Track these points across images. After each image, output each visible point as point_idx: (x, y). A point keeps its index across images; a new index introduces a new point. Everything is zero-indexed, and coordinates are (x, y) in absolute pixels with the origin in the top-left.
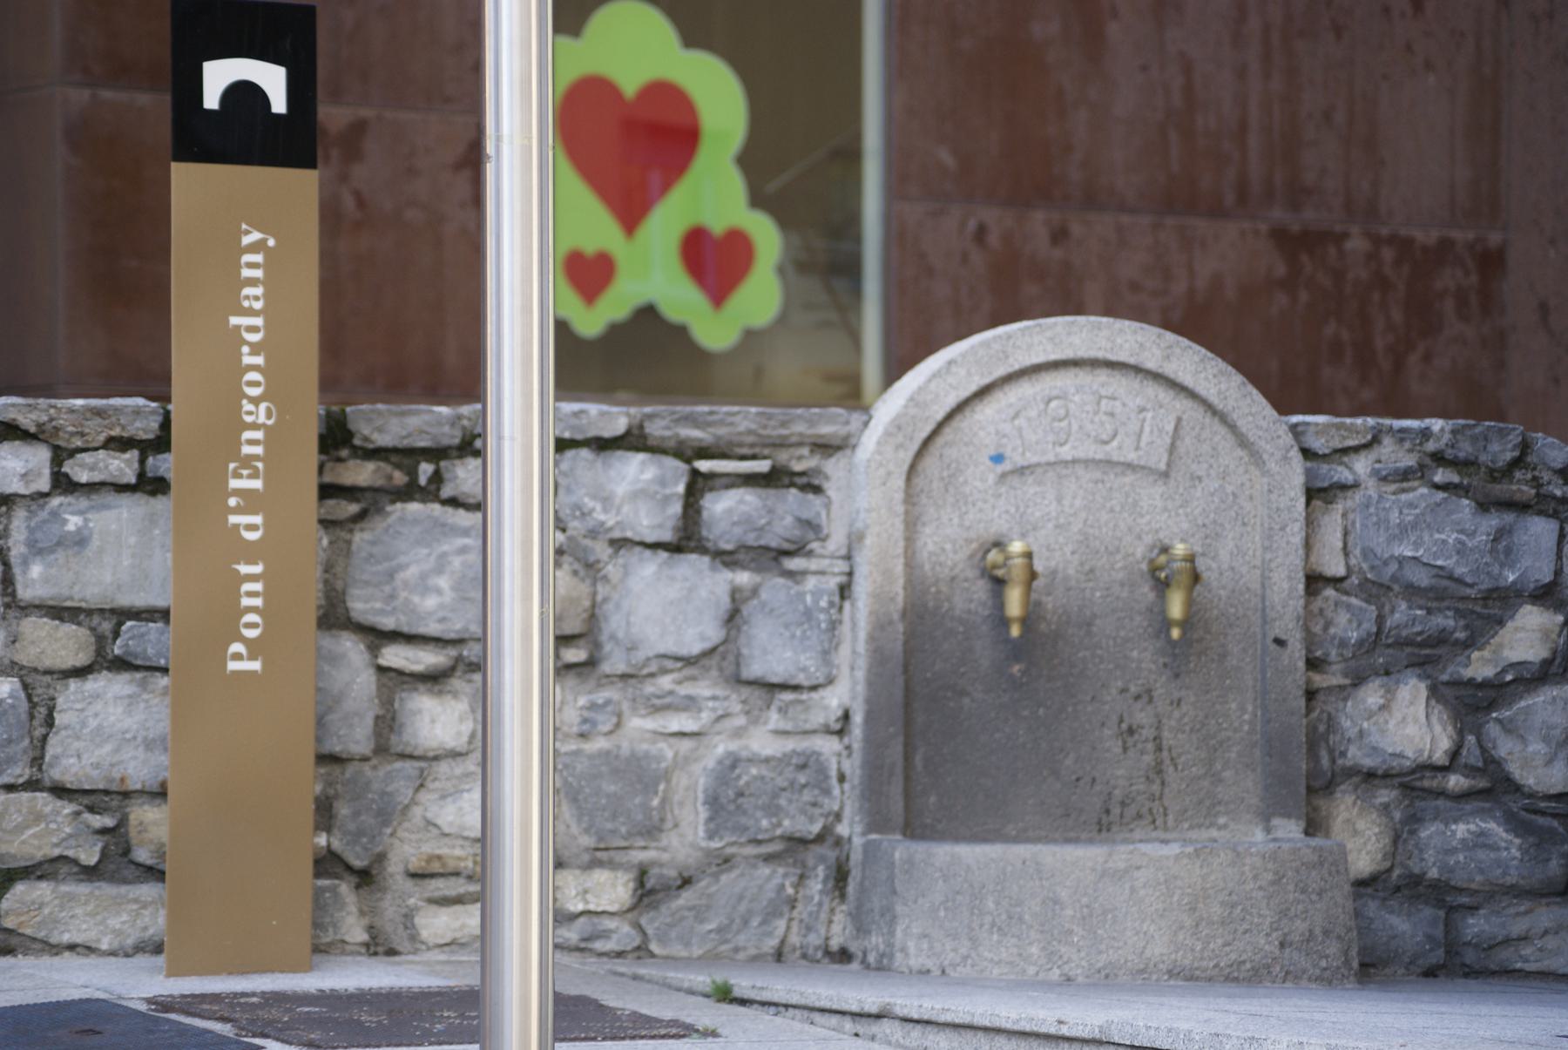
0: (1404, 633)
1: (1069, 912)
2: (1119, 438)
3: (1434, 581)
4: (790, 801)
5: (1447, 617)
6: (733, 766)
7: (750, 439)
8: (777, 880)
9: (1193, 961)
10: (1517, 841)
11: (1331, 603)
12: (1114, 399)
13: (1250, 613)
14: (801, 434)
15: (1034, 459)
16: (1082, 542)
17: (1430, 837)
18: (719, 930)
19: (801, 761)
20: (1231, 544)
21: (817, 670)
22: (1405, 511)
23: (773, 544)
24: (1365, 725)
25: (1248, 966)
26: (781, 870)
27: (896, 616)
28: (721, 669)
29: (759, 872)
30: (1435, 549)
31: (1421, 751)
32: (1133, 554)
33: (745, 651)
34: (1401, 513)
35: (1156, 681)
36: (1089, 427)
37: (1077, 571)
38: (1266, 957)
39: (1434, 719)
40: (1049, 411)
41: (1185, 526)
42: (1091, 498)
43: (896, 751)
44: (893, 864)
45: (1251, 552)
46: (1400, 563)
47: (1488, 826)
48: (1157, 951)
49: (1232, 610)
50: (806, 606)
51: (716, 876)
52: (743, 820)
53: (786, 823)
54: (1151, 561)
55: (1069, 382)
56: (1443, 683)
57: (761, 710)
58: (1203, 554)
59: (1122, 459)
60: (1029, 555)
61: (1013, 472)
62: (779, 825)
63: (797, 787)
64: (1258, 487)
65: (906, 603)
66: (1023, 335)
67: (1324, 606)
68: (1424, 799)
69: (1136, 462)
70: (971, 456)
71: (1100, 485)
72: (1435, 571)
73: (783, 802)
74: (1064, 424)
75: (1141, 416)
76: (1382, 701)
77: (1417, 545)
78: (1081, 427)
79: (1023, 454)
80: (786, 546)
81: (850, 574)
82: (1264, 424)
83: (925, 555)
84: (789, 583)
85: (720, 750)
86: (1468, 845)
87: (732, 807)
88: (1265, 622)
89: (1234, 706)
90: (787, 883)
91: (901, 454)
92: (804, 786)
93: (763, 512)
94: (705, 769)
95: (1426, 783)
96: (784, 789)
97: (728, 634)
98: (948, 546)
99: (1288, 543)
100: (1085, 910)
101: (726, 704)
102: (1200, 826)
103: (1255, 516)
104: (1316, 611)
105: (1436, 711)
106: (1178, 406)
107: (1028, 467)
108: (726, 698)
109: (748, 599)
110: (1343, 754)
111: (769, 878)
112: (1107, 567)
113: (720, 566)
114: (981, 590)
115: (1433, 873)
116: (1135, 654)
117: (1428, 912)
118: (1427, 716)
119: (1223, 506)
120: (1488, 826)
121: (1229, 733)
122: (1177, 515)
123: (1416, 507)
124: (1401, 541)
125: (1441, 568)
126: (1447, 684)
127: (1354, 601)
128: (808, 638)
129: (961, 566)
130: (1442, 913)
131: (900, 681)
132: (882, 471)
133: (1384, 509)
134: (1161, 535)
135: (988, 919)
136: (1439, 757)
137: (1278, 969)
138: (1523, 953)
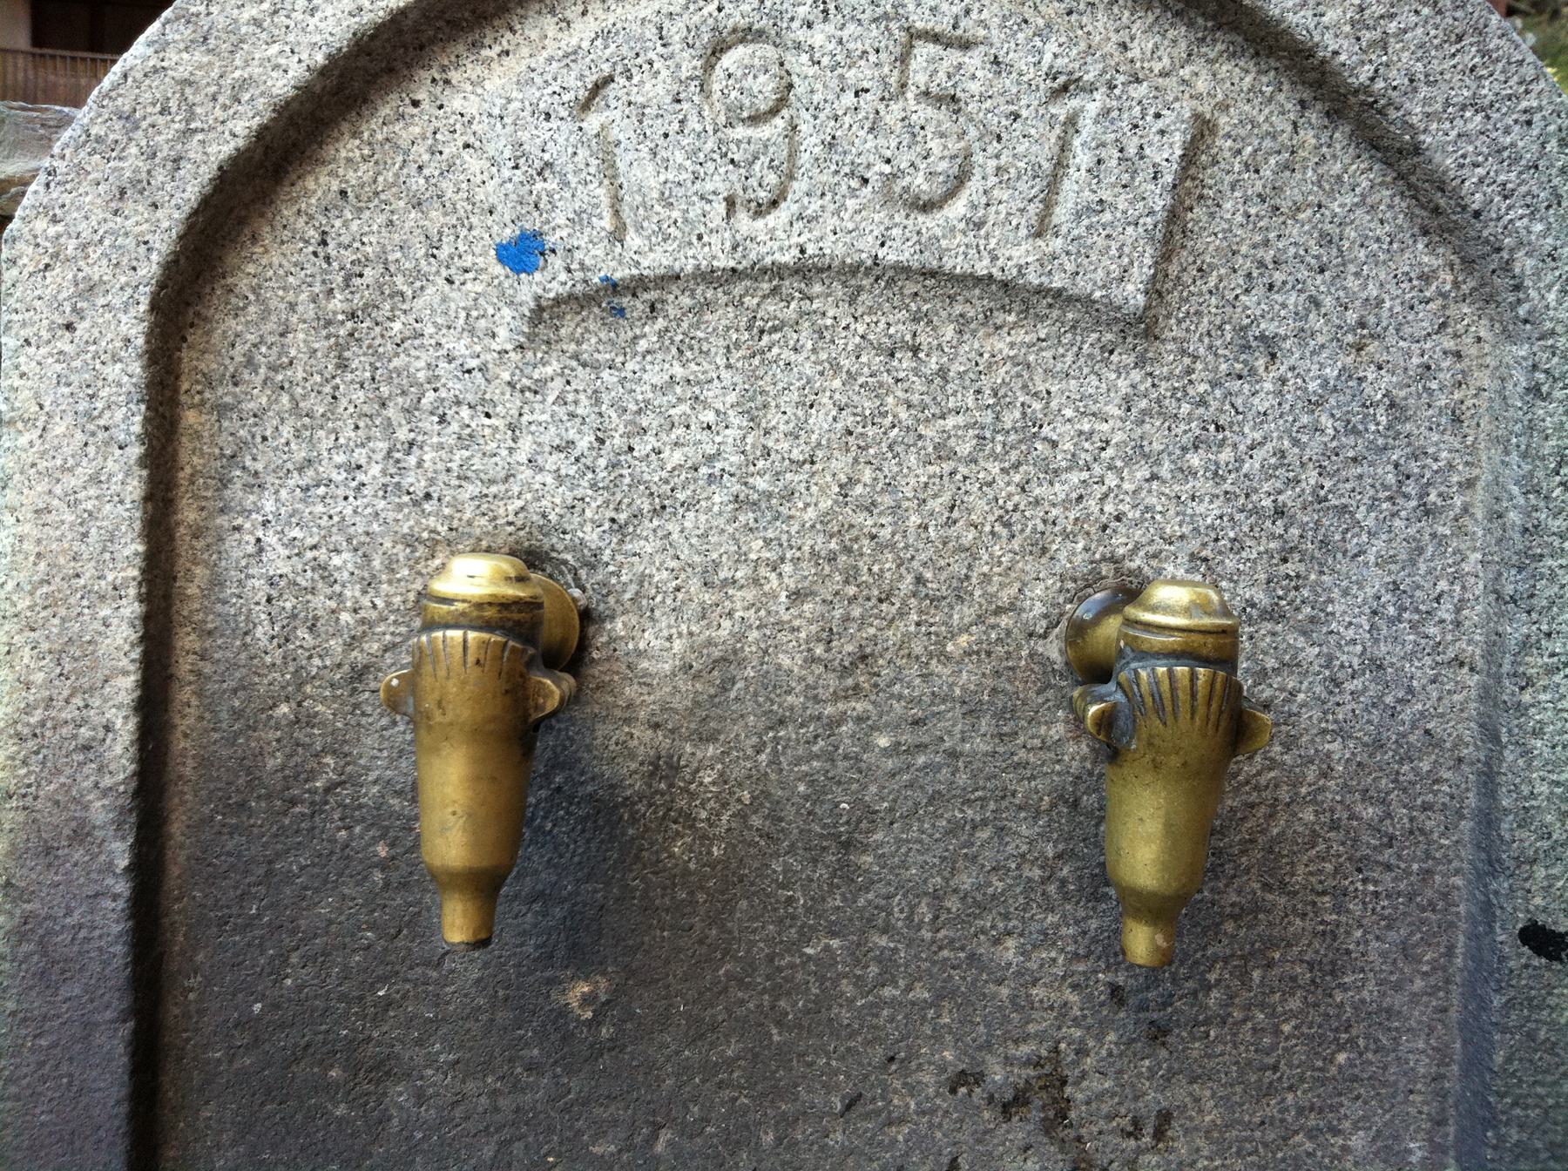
2: (974, 186)
12: (966, 45)
13: (1431, 823)
15: (656, 260)
16: (832, 558)
20: (1376, 581)
27: (100, 812)
32: (1012, 607)
35: (1082, 1052)
37: (813, 660)
40: (717, 83)
41: (1209, 511)
42: (868, 405)
45: (1445, 612)
49: (1370, 812)
54: (1078, 631)
58: (1272, 614)
59: (982, 268)
64: (1483, 379)
69: (1033, 279)
70: (433, 246)
71: (904, 361)
74: (764, 132)
75: (1061, 110)
79: (617, 235)
82: (1526, 143)
88: (1490, 865)
89: (1358, 1141)
91: (136, 216)
103: (1470, 484)
106: (1202, 85)
107: (637, 285)
116: (1010, 951)
119: (1352, 446)
129: (386, 632)
131: (114, 1043)
132: (62, 277)
134: (1120, 544)
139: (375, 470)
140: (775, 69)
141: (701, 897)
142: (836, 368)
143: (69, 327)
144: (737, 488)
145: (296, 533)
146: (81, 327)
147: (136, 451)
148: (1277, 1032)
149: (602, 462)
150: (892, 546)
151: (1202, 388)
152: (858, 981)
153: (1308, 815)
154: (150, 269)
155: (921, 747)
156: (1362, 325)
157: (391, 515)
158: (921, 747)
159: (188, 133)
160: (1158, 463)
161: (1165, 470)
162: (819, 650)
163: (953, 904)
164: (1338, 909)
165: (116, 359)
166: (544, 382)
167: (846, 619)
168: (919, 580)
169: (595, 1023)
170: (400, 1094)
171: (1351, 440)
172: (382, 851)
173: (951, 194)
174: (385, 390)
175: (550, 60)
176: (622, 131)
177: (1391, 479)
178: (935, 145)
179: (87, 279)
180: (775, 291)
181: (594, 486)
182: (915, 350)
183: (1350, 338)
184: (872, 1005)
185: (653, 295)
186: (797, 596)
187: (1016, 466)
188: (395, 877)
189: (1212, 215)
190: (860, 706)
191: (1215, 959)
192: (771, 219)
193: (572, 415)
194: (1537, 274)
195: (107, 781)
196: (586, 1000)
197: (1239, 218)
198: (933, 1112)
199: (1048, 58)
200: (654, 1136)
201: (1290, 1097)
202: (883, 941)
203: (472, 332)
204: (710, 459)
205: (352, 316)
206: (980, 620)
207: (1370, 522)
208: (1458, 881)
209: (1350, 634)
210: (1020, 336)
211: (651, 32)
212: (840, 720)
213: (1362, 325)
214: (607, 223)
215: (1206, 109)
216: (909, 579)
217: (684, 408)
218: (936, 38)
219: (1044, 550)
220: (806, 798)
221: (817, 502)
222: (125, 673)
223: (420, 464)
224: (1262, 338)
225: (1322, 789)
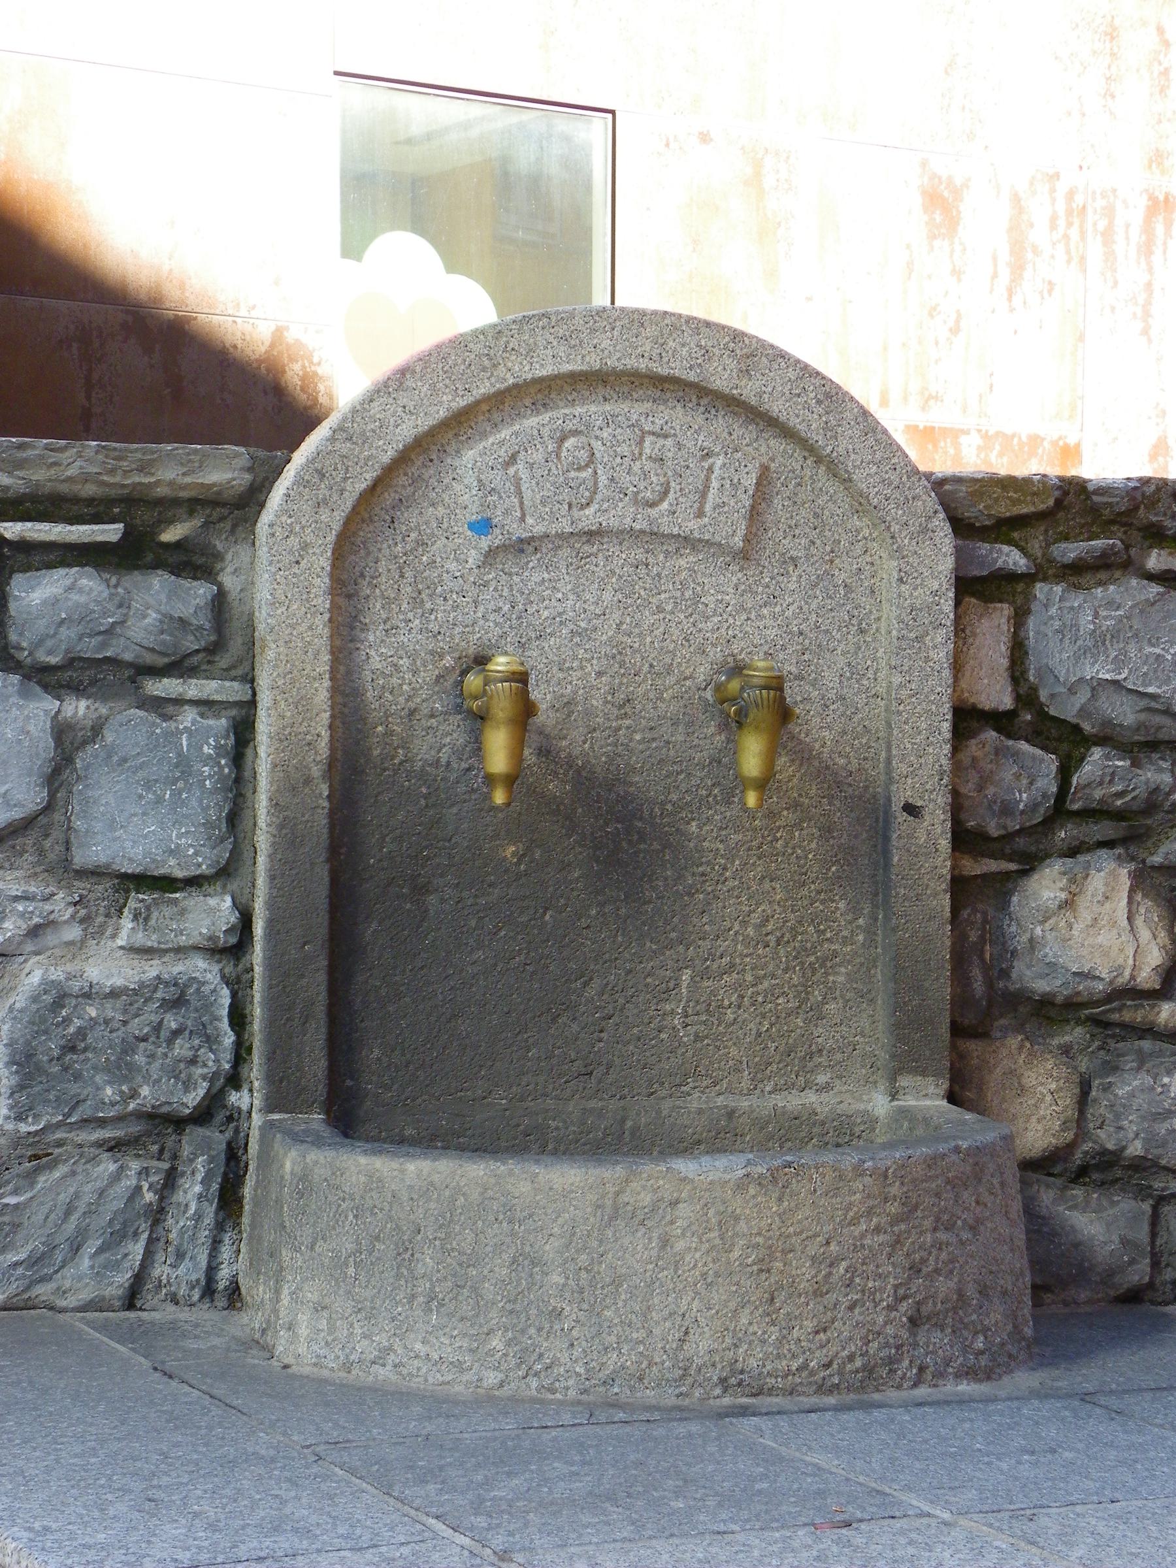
0: (1098, 794)
1: (557, 1278)
2: (671, 496)
3: (1143, 717)
4: (152, 1056)
5: (1161, 770)
6: (58, 1004)
7: (90, 490)
8: (129, 1181)
9: (764, 1360)
12: (666, 436)
14: (171, 483)
15: (539, 530)
17: (1132, 1095)
18: (35, 1261)
19: (171, 993)
20: (841, 662)
21: (196, 854)
22: (1103, 613)
23: (128, 656)
24: (1038, 931)
25: (858, 1363)
26: (135, 1165)
27: (316, 771)
28: (41, 852)
29: (101, 1168)
31: (1120, 969)
33: (78, 824)
34: (1096, 615)
36: (625, 480)
38: (887, 1345)
39: (1139, 921)
41: (772, 633)
43: (316, 984)
44: (282, 1177)
45: (870, 675)
46: (1093, 689)
48: (704, 1346)
49: (842, 761)
50: (180, 754)
51: (30, 1177)
52: (74, 1088)
53: (145, 1091)
54: (719, 688)
55: (593, 408)
56: (1153, 867)
57: (108, 916)
58: (799, 677)
59: (676, 531)
60: (521, 678)
61: (504, 548)
62: (134, 1094)
63: (164, 1034)
65: (333, 749)
66: (520, 331)
67: (979, 754)
68: (1123, 1039)
69: (696, 535)
71: (642, 571)
72: (1143, 703)
73: (140, 1059)
74: (584, 474)
75: (706, 465)
76: (1063, 896)
77: (1119, 663)
78: (612, 479)
79: (523, 519)
80: (149, 659)
81: (252, 703)
82: (893, 476)
83: (367, 673)
84: (153, 718)
85: (36, 978)
87: (55, 1069)
89: (842, 905)
90: (146, 1186)
91: (325, 516)
92: (176, 1033)
93: (110, 606)
94: (11, 1009)
95: (1127, 1016)
96: (144, 1039)
97: (52, 795)
98: (404, 662)
99: (927, 659)
100: (583, 1274)
101: (48, 907)
102: (788, 1087)
103: (879, 619)
105: (1142, 911)
108: (47, 898)
109: (85, 743)
110: (1005, 974)
111: (117, 1177)
112: (652, 695)
113: (38, 689)
114: (454, 733)
115: (1136, 1149)
121: (836, 947)
122: (760, 617)
123: (1118, 609)
125: (1153, 697)
126: (1160, 868)
127: (1024, 746)
128: (183, 803)
130: (1146, 1207)
131: (322, 873)
132: (294, 542)
133: (1072, 608)
134: (735, 648)
135: (423, 1286)
136: (1147, 977)
137: (906, 1363)
139: (417, 622)
140: (587, 448)
141: (562, 808)
142: (613, 572)
143: (297, 562)
144: (572, 627)
145: (383, 650)
146: (303, 563)
147: (327, 616)
148: (806, 857)
149: (514, 616)
150: (639, 651)
151: (767, 580)
152: (630, 842)
153: (816, 763)
154: (331, 538)
155: (654, 739)
156: (832, 552)
157: (424, 642)
158: (654, 739)
159: (345, 479)
160: (750, 613)
161: (753, 616)
162: (609, 698)
163: (669, 807)
164: (830, 804)
165: (319, 576)
166: (488, 582)
167: (621, 684)
168: (651, 666)
169: (518, 863)
170: (432, 899)
171: (829, 601)
172: (424, 790)
173: (662, 500)
174: (420, 586)
175: (493, 444)
176: (524, 475)
177: (846, 617)
178: (654, 479)
179: (305, 542)
180: (588, 541)
181: (511, 627)
182: (647, 565)
183: (827, 558)
184: (635, 852)
185: (537, 544)
186: (599, 674)
187: (691, 615)
188: (431, 801)
189: (769, 506)
190: (628, 722)
191: (779, 827)
192: (587, 512)
193: (501, 596)
194: (900, 531)
195: (318, 758)
196: (514, 854)
197: (780, 507)
198: (663, 897)
199: (700, 442)
200: (545, 913)
201: (813, 887)
202: (639, 824)
203: (457, 561)
204: (560, 614)
205: (405, 554)
206: (678, 682)
207: (838, 636)
208: (879, 790)
209: (831, 685)
210: (691, 559)
211: (535, 432)
212: (619, 729)
213: (832, 552)
214: (518, 514)
215: (765, 460)
216: (647, 665)
217: (549, 592)
218: (654, 434)
219: (704, 652)
220: (606, 763)
222: (325, 711)
223: (436, 618)
224: (791, 558)
225: (822, 753)
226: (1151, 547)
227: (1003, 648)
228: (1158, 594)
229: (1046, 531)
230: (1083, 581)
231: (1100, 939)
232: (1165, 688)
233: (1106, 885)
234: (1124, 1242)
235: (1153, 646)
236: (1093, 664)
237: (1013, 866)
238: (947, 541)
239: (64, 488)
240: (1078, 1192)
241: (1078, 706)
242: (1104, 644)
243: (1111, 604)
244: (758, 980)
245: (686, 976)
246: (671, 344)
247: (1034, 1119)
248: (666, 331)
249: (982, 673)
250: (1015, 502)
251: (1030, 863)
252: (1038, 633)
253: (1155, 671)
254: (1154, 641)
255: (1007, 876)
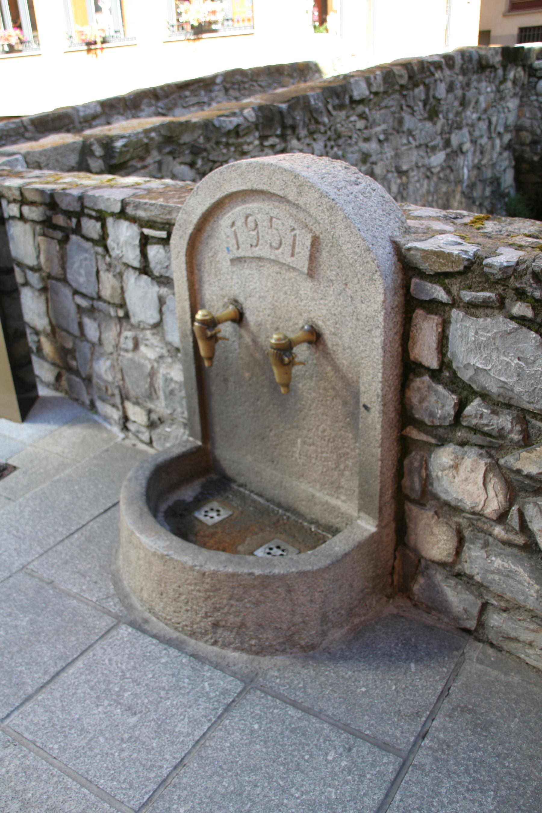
0: (474, 422)
2: (283, 246)
3: (501, 390)
10: (537, 587)
11: (426, 384)
17: (477, 557)
20: (350, 331)
22: (481, 333)
24: (440, 474)
30: (500, 367)
31: (477, 504)
34: (476, 333)
39: (490, 487)
41: (324, 312)
46: (475, 370)
47: (516, 568)
75: (293, 233)
77: (487, 360)
79: (238, 248)
82: (358, 251)
86: (498, 572)
89: (351, 435)
95: (480, 524)
99: (373, 342)
104: (416, 387)
117: (471, 598)
118: (485, 484)
120: (516, 568)
121: (348, 451)
123: (488, 332)
124: (476, 354)
127: (440, 388)
133: (466, 326)
134: (312, 315)
138: (527, 651)
161: (318, 303)
221: (269, 299)
226: (517, 300)
227: (434, 338)
228: (513, 328)
229: (461, 282)
230: (478, 312)
231: (468, 488)
232: (509, 380)
233: (472, 465)
234: (465, 610)
235: (505, 356)
236: (474, 358)
237: (433, 441)
238: (381, 286)
239: (154, 219)
240: (452, 582)
241: (469, 376)
242: (480, 348)
243: (485, 329)
244: (322, 452)
245: (299, 441)
246: (274, 179)
247: (436, 547)
248: (272, 172)
249: (425, 348)
250: (443, 265)
251: (442, 442)
252: (453, 334)
253: (506, 370)
254: (506, 354)
255: (431, 444)
